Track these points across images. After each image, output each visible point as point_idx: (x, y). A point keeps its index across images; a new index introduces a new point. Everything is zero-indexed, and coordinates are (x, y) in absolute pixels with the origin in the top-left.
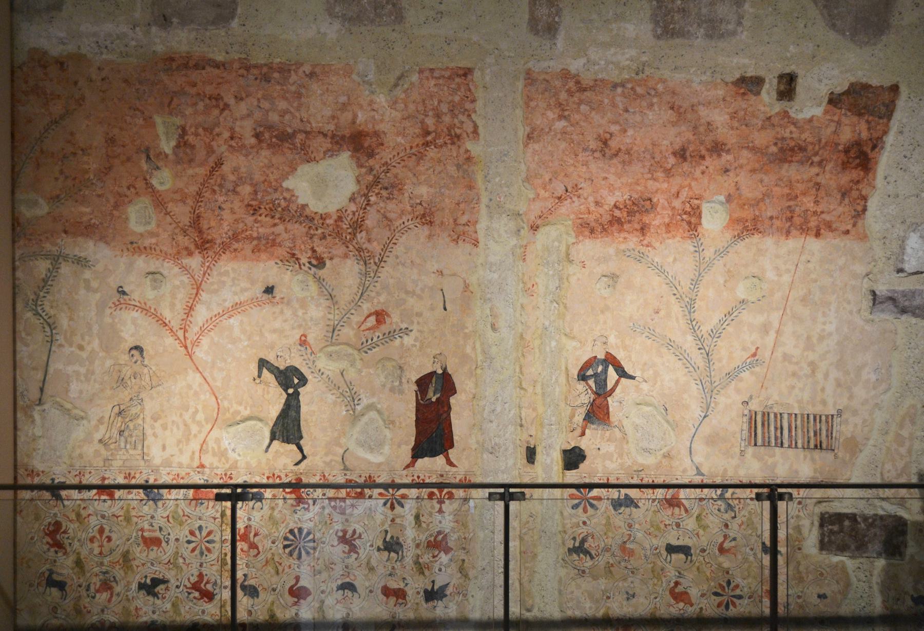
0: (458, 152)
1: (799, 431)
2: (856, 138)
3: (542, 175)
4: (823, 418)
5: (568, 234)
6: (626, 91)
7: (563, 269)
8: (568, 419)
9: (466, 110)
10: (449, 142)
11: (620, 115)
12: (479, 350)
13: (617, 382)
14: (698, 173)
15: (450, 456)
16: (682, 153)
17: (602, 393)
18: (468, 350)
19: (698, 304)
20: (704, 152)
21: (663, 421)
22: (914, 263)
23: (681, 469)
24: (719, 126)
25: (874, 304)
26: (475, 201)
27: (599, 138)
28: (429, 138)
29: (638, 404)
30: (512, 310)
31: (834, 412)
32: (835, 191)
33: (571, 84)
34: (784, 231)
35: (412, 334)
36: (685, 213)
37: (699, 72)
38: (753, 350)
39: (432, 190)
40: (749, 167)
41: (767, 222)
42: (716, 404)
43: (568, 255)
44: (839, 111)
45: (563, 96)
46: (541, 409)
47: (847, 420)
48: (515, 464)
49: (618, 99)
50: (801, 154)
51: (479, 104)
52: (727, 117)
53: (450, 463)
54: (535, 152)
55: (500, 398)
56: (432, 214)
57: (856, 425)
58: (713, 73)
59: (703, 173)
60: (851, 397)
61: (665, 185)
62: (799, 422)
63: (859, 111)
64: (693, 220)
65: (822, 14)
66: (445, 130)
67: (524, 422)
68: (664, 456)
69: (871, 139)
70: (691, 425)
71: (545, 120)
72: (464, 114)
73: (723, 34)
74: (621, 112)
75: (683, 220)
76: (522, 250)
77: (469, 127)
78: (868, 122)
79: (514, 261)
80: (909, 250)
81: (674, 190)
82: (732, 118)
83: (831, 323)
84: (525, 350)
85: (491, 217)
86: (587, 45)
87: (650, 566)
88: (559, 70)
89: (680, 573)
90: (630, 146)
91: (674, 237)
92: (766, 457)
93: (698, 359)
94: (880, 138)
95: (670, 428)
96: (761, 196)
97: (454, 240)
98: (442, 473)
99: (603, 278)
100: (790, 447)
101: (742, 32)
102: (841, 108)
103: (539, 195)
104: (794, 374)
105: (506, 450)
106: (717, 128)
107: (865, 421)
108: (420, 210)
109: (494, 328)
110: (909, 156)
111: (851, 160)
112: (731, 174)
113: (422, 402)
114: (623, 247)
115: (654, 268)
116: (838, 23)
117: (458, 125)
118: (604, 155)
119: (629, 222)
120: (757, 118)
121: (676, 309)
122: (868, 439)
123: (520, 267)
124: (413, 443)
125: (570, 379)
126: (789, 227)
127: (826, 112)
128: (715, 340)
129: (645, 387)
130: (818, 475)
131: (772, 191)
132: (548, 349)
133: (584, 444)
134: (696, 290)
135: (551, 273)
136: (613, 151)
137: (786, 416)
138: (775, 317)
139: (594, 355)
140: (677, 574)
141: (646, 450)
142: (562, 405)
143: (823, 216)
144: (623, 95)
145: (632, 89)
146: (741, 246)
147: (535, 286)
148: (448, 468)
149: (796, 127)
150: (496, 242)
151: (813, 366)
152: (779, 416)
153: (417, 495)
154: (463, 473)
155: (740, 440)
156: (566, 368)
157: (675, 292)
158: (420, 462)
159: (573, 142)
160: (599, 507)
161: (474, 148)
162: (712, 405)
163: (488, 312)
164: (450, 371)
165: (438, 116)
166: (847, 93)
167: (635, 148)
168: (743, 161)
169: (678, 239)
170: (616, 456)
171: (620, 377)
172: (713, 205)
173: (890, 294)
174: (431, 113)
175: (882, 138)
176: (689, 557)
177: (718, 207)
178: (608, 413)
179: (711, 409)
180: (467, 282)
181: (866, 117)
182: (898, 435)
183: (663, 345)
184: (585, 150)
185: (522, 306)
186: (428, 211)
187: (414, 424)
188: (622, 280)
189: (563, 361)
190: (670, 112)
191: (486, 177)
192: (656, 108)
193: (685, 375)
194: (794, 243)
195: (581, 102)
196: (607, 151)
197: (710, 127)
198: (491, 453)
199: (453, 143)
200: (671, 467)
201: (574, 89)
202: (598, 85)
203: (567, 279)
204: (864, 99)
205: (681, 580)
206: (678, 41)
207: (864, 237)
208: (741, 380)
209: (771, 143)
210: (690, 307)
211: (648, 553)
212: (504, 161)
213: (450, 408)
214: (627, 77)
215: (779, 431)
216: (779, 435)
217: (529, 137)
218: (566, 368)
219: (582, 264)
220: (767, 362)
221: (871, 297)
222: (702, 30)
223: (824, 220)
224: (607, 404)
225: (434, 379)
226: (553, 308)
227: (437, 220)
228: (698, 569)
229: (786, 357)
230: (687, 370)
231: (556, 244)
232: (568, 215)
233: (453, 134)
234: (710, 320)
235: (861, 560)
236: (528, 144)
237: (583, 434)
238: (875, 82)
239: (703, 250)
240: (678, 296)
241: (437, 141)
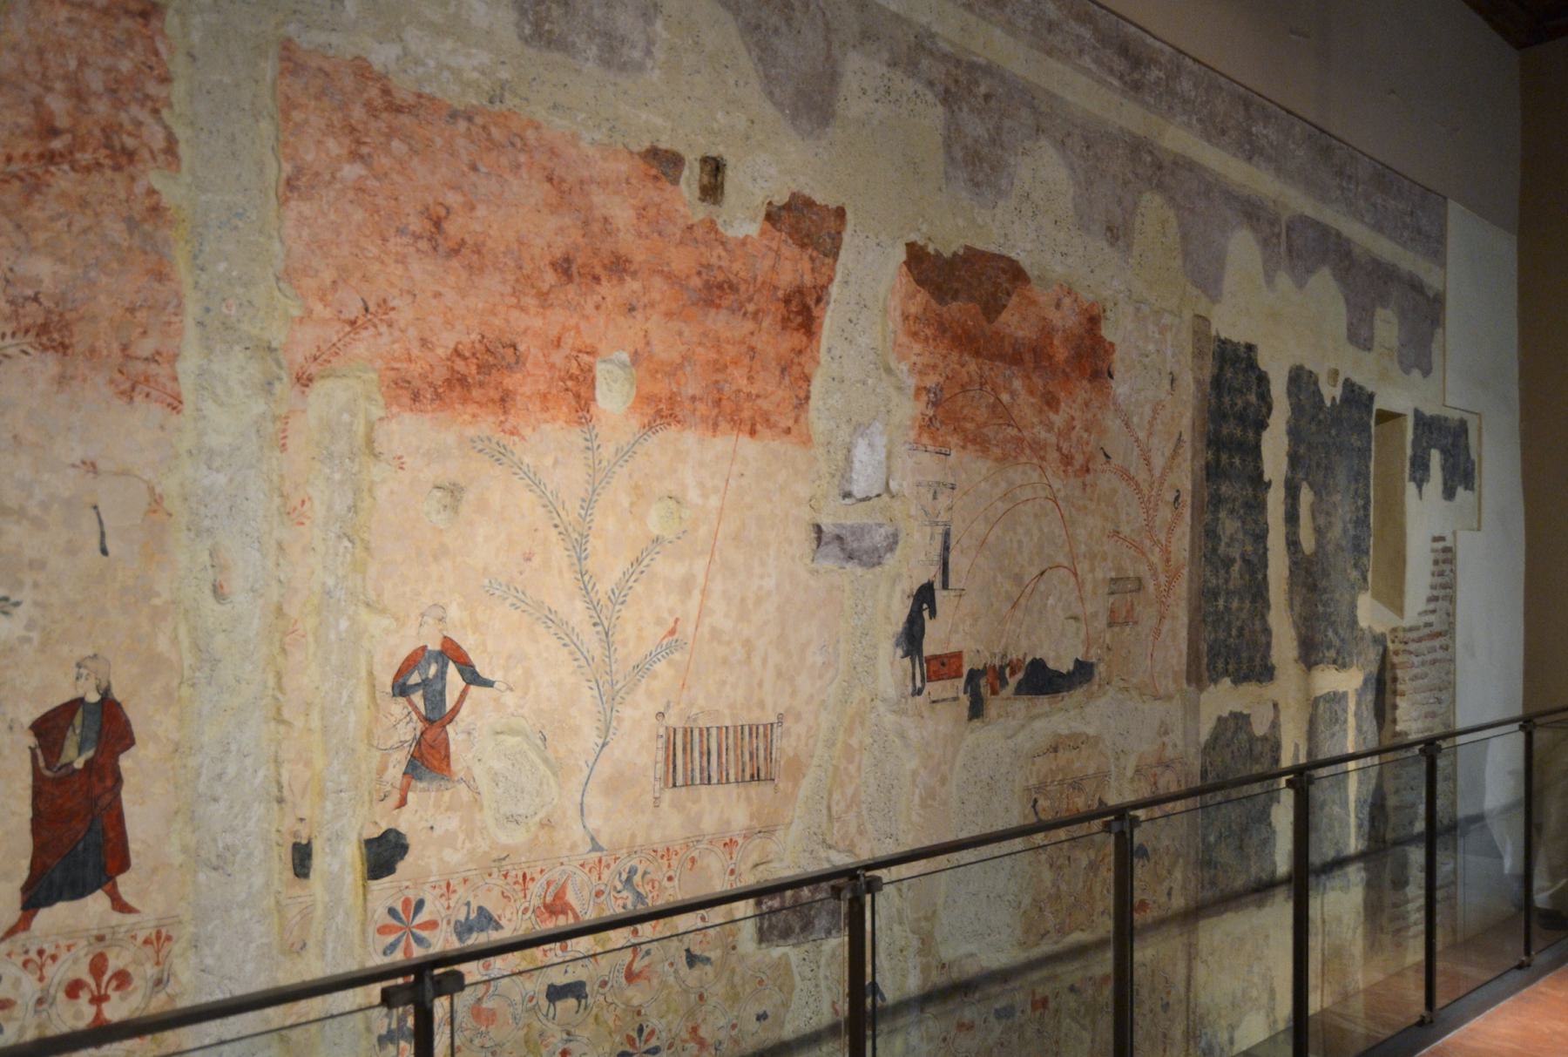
0: (130, 192)
1: (731, 754)
2: (798, 282)
3: (317, 271)
4: (761, 729)
5: (369, 398)
6: (473, 129)
7: (360, 472)
8: (374, 776)
9: (147, 97)
10: (107, 162)
11: (464, 174)
12: (185, 642)
13: (463, 694)
14: (589, 308)
15: (122, 889)
16: (565, 265)
17: (437, 718)
18: (163, 644)
19: (594, 543)
20: (598, 270)
21: (538, 761)
22: (863, 485)
23: (568, 844)
24: (621, 226)
25: (818, 546)
26: (170, 309)
27: (426, 212)
28: (57, 144)
29: (497, 733)
30: (258, 555)
31: (774, 719)
32: (774, 364)
33: (373, 92)
34: (711, 422)
35: (19, 611)
36: (571, 378)
37: (590, 123)
38: (671, 624)
39: (64, 271)
40: (663, 308)
41: (687, 403)
42: (620, 720)
43: (370, 441)
44: (778, 234)
45: (358, 113)
46: (319, 762)
47: (788, 729)
48: (267, 885)
49: (461, 142)
50: (732, 297)
51: (178, 90)
52: (632, 213)
53: (120, 906)
54: (302, 220)
55: (234, 747)
56: (66, 326)
57: (799, 736)
58: (610, 130)
59: (598, 307)
60: (794, 694)
61: (538, 323)
62: (731, 741)
63: (804, 240)
64: (583, 391)
65: (757, 71)
66: (97, 132)
67: (286, 792)
68: (542, 825)
69: (814, 287)
70: (582, 763)
71: (323, 155)
72: (143, 106)
73: (625, 64)
74: (466, 169)
75: (567, 390)
76: (279, 425)
77: (159, 142)
78: (812, 259)
79: (261, 448)
80: (857, 465)
81: (554, 332)
82: (640, 217)
83: (769, 576)
84: (287, 639)
85: (209, 350)
86: (403, 20)
87: (522, 1033)
88: (349, 57)
89: (569, 1034)
90: (481, 238)
91: (554, 419)
92: (689, 804)
93: (591, 641)
94: (824, 288)
95: (549, 773)
96: (679, 361)
97: (123, 393)
98: (102, 932)
99: (435, 491)
100: (719, 782)
101: (653, 68)
102: (780, 230)
103: (311, 311)
104: (725, 661)
105: (250, 855)
106: (618, 230)
107: (810, 728)
108: (33, 313)
109: (218, 592)
110: (855, 320)
111: (792, 316)
112: (639, 315)
113: (48, 773)
114: (471, 431)
115: (522, 475)
116: (777, 91)
117: (130, 128)
118: (435, 249)
119: (481, 385)
120: (675, 224)
121: (560, 554)
122: (812, 757)
123: (274, 462)
124: (25, 874)
125: (378, 695)
126: (717, 416)
127: (763, 233)
128: (618, 607)
129: (510, 699)
130: (754, 823)
131: (694, 352)
132: (333, 636)
133: (405, 822)
134: (588, 519)
135: (337, 477)
136: (451, 244)
137: (714, 732)
138: (700, 565)
139: (421, 644)
140: (565, 1036)
141: (514, 819)
142: (362, 748)
143: (759, 401)
144: (468, 135)
145: (484, 127)
146: (653, 440)
147: (307, 504)
148: (117, 918)
149: (726, 250)
150: (222, 405)
151: (748, 644)
152: (705, 732)
153: (38, 995)
154: (152, 923)
155: (652, 779)
156: (370, 673)
157: (557, 521)
158: (46, 918)
159: (378, 211)
160: (433, 941)
161: (172, 190)
162: (614, 724)
163: (205, 558)
164: (118, 694)
165: (78, 95)
166: (787, 207)
167: (490, 243)
168: (657, 296)
169: (560, 423)
170: (461, 837)
171: (469, 684)
172: (609, 367)
173: (837, 531)
174: (59, 86)
175: (827, 287)
176: (583, 1001)
177: (618, 372)
178: (447, 756)
179: (611, 730)
180: (158, 490)
181: (810, 251)
182: (848, 747)
183: (538, 619)
184: (400, 232)
185: (280, 547)
186: (55, 318)
187: (27, 826)
188: (470, 496)
189: (363, 658)
190: (547, 186)
191: (195, 257)
192: (524, 172)
193: (574, 673)
194: (722, 443)
195: (391, 133)
196: (440, 240)
197: (609, 227)
198: (215, 869)
199: (117, 168)
200: (553, 844)
201: (379, 102)
202: (421, 105)
203: (370, 490)
204: (808, 222)
205: (570, 1046)
206: (557, 56)
207: (807, 441)
208: (655, 676)
209: (694, 271)
210: (579, 548)
211: (520, 1007)
212: (236, 228)
213: (118, 780)
214: (474, 102)
215: (705, 758)
216: (705, 764)
217: (290, 184)
218: (370, 673)
219: (397, 462)
220: (690, 642)
221: (814, 535)
222: (594, 48)
223: (760, 409)
224: (446, 740)
225: (78, 720)
226: (341, 550)
227: (80, 338)
228: (596, 1018)
229: (715, 634)
230: (576, 663)
231: (346, 417)
232: (371, 361)
233: (118, 146)
234: (610, 570)
235: (807, 946)
236: (287, 200)
237: (403, 802)
238: (819, 198)
239: (599, 446)
240: (561, 529)
241: (78, 156)
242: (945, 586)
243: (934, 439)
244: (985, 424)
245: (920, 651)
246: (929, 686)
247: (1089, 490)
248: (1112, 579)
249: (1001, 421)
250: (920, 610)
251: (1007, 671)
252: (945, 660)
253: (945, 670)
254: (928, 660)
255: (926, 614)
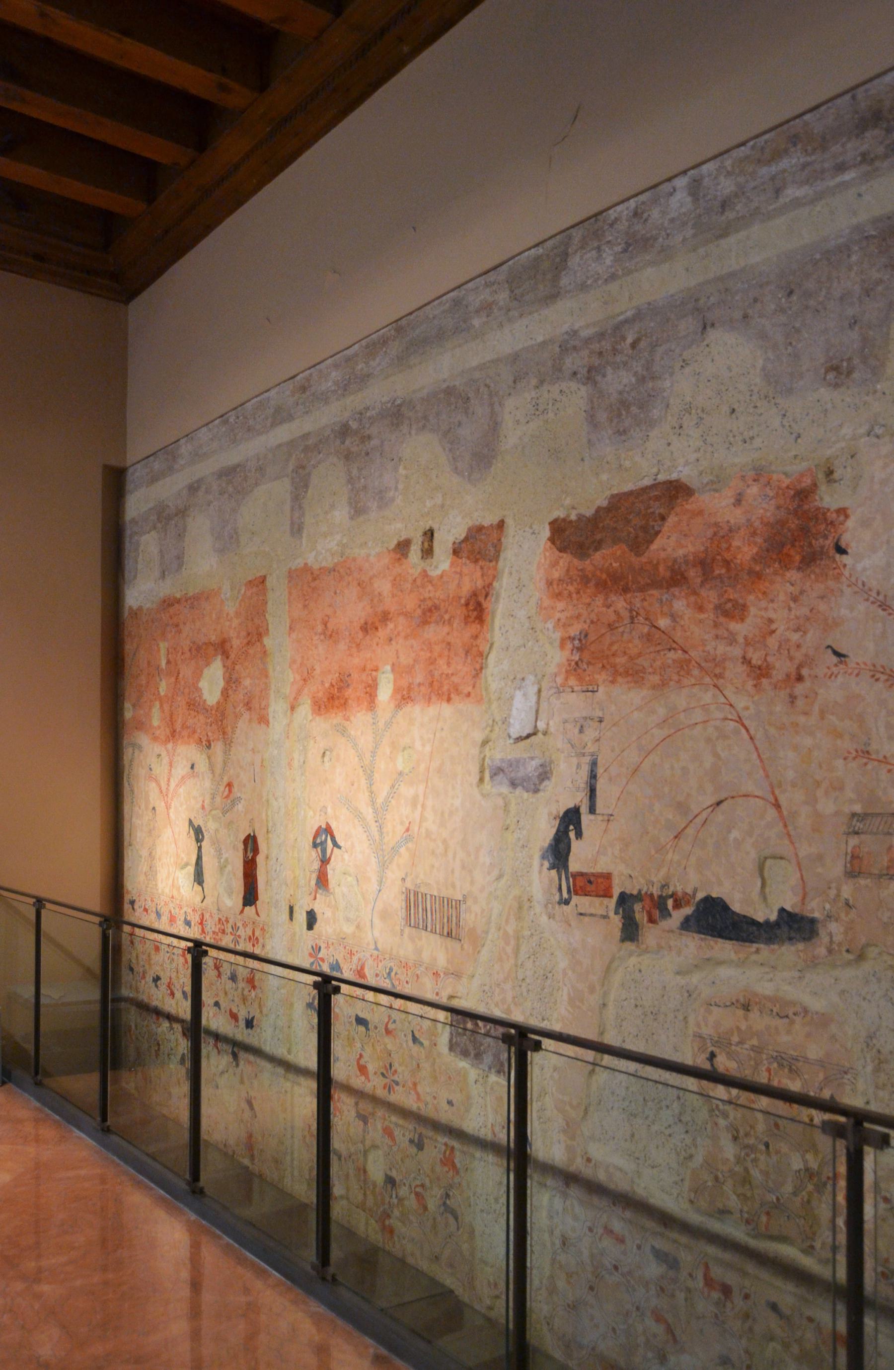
4: (454, 903)
19: (376, 776)
31: (460, 898)
40: (403, 634)
60: (472, 882)
78: (482, 568)
94: (490, 585)
107: (483, 911)
112: (393, 642)
121: (363, 782)
138: (421, 788)
164: (256, 834)
210: (370, 777)
229: (428, 834)
237: (315, 899)
242: (592, 810)
243: (580, 679)
244: (640, 655)
245: (566, 866)
246: (575, 899)
247: (800, 703)
248: (854, 815)
249: (658, 648)
250: (566, 832)
251: (670, 902)
252: (592, 879)
253: (592, 888)
254: (576, 876)
255: (572, 835)
